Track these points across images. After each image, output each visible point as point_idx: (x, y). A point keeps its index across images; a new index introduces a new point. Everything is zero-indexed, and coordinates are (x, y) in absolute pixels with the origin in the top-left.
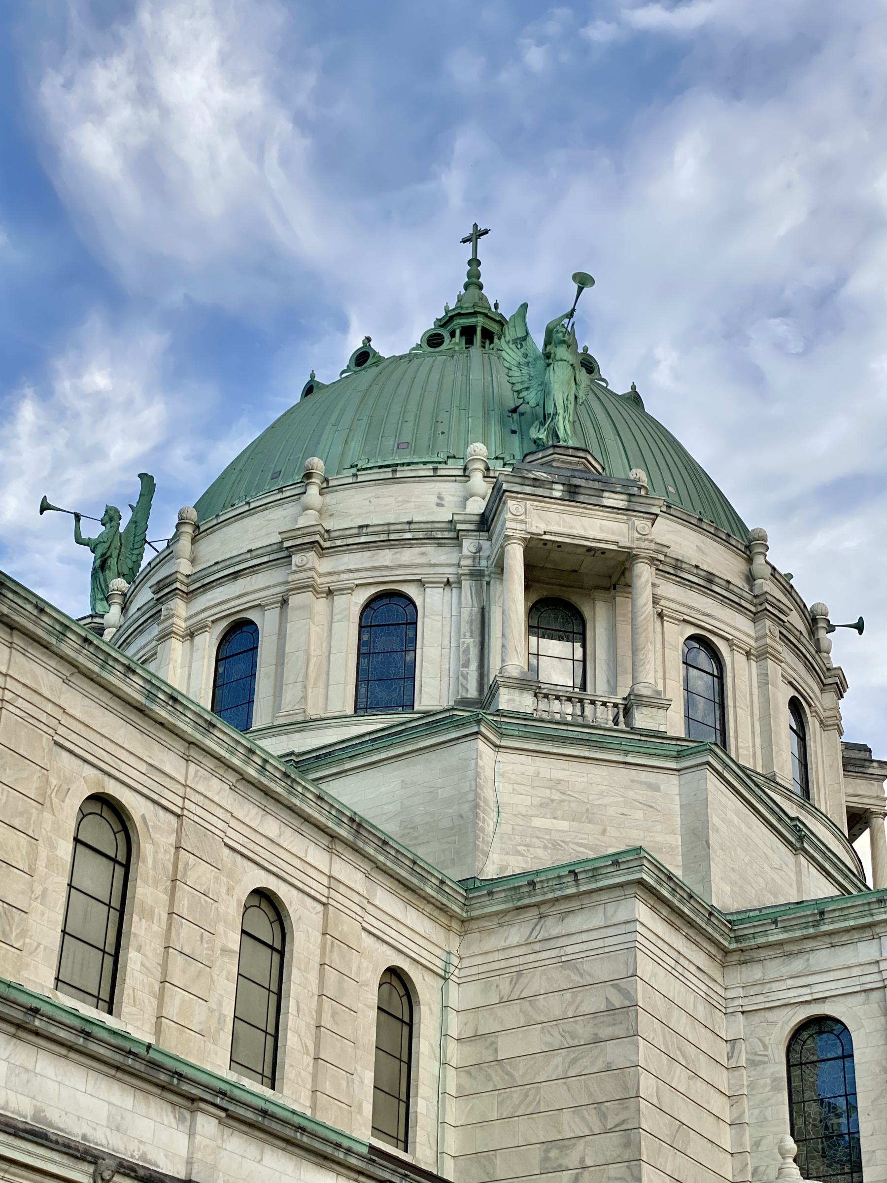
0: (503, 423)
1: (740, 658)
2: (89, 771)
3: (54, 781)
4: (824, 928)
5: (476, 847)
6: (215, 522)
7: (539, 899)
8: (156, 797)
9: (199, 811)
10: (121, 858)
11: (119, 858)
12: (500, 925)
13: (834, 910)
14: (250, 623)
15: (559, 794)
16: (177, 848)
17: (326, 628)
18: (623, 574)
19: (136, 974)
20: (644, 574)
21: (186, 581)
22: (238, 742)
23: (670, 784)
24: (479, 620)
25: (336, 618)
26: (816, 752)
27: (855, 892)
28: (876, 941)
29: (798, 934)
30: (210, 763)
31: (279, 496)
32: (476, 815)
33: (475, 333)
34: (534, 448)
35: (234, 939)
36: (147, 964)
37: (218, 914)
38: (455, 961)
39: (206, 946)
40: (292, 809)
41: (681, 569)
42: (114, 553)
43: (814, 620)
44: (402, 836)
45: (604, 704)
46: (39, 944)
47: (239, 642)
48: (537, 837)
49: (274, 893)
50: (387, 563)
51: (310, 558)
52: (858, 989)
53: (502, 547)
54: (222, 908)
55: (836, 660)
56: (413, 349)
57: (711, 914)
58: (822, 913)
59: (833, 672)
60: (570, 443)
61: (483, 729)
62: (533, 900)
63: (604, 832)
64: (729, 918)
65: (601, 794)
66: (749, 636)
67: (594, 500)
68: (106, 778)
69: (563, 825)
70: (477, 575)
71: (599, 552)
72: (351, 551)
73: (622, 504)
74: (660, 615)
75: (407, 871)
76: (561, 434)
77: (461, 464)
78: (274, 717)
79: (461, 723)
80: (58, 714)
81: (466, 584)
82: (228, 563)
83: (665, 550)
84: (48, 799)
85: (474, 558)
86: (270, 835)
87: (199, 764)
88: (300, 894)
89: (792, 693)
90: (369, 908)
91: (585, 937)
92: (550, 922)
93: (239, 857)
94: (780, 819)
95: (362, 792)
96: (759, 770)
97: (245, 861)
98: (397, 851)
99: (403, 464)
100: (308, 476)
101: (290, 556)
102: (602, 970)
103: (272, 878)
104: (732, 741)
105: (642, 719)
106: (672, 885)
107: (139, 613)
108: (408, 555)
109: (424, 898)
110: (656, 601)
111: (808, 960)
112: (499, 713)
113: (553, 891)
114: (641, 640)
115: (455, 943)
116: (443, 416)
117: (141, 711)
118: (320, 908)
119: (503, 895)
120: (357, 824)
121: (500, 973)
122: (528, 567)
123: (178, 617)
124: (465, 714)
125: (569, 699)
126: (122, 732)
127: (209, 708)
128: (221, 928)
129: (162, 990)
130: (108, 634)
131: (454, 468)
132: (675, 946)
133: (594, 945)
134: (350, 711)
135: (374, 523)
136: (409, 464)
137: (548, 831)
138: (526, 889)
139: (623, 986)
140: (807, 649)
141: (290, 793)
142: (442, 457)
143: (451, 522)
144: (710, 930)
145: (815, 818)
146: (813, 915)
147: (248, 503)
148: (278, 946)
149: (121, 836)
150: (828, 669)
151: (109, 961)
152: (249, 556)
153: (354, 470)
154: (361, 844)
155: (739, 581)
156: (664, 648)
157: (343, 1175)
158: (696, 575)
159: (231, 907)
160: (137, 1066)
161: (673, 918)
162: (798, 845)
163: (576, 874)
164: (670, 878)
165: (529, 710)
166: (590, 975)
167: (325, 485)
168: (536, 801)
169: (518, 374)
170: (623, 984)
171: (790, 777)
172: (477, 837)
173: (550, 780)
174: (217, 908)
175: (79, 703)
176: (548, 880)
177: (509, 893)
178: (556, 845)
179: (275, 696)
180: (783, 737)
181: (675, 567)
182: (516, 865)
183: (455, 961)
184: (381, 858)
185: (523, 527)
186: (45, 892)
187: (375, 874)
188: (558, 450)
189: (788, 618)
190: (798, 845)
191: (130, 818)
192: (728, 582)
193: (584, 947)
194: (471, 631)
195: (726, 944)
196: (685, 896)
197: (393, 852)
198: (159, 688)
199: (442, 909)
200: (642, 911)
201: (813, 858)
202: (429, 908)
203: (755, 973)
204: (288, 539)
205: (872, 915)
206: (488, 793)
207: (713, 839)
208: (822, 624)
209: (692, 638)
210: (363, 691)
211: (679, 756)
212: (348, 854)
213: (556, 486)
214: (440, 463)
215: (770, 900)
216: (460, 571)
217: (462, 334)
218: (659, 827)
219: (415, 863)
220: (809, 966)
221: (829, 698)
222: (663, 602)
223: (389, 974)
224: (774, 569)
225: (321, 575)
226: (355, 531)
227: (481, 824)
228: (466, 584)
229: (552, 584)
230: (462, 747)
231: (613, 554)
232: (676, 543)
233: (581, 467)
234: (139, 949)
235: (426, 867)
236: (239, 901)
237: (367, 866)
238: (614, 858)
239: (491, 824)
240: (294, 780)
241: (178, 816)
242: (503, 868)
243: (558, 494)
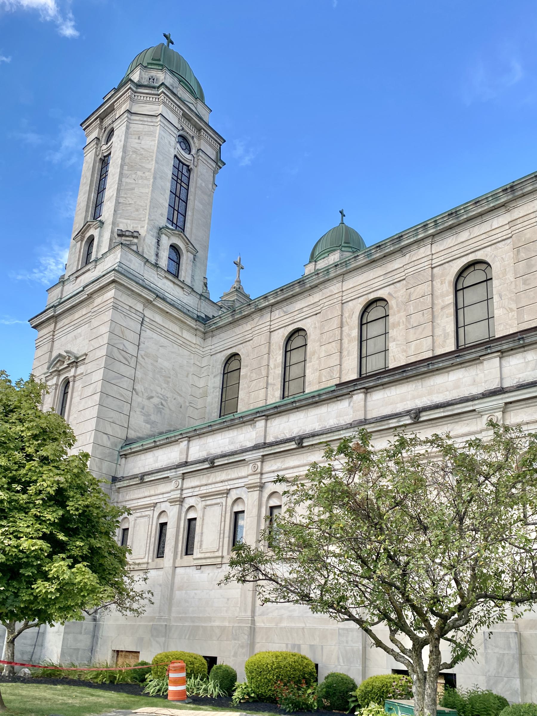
157: (330, 403)
160: (228, 424)
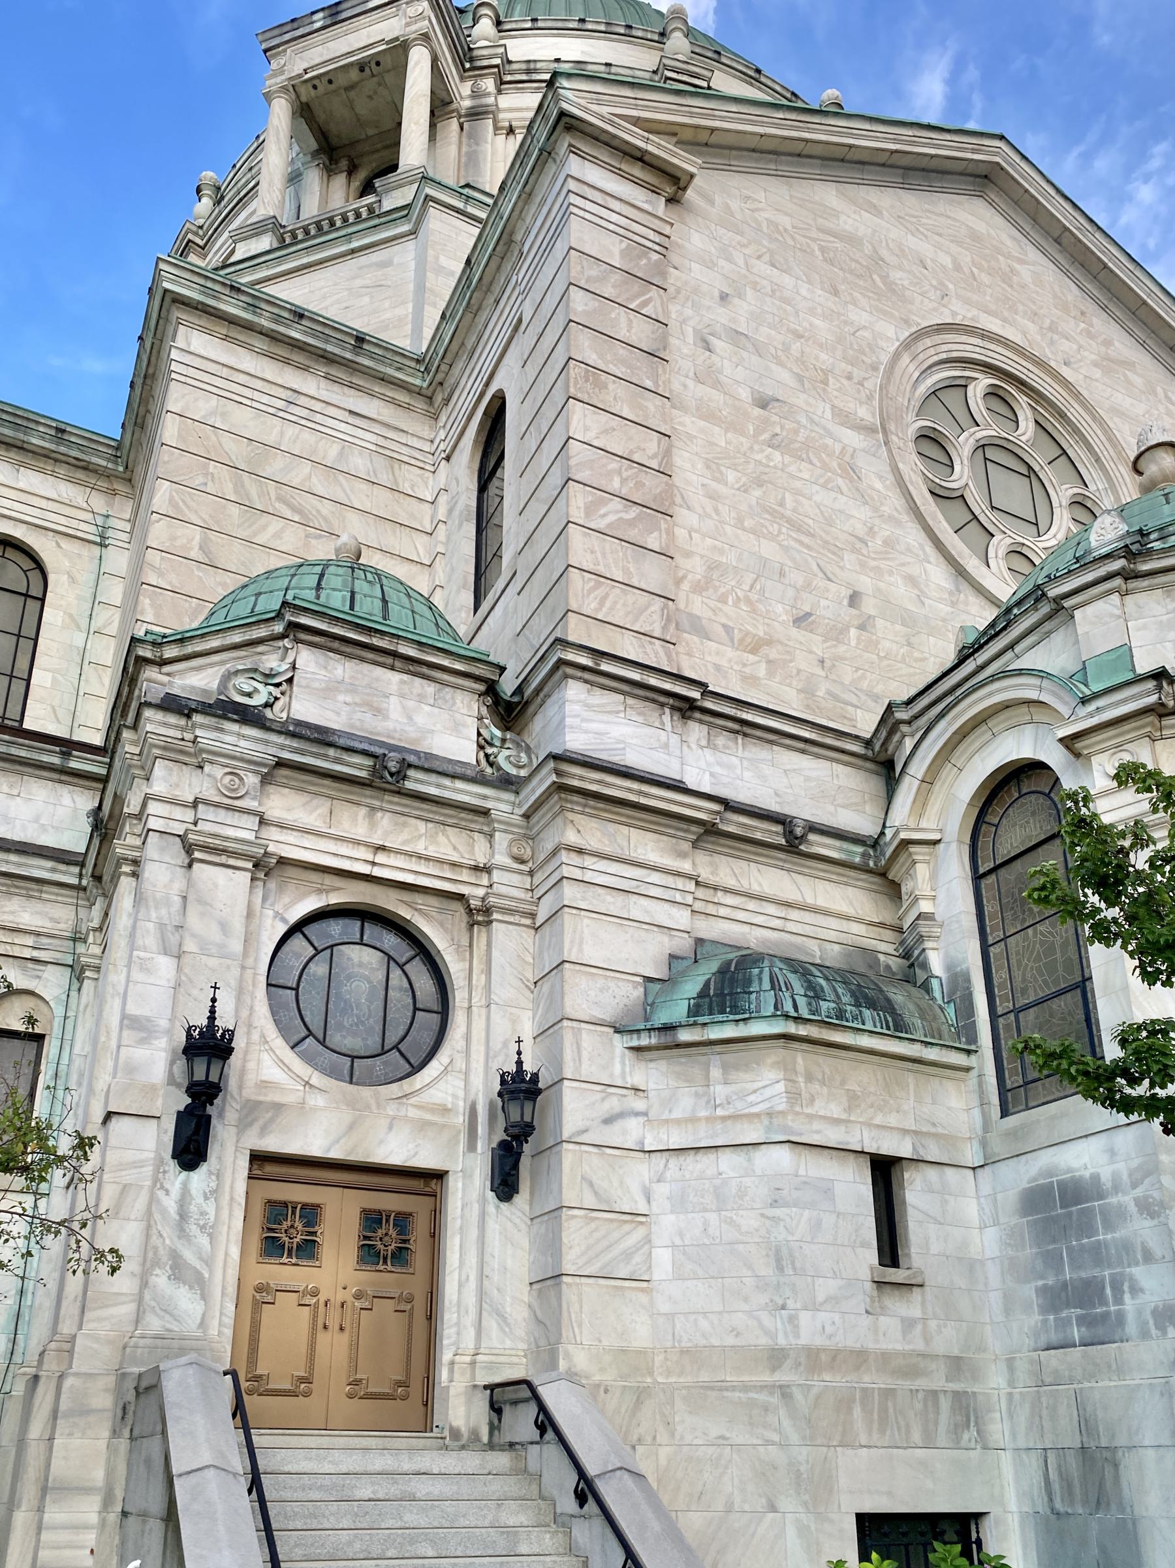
41: (536, 71)
71: (373, 65)
144: (367, 362)
181: (528, 71)
195: (418, 382)
229: (378, 151)
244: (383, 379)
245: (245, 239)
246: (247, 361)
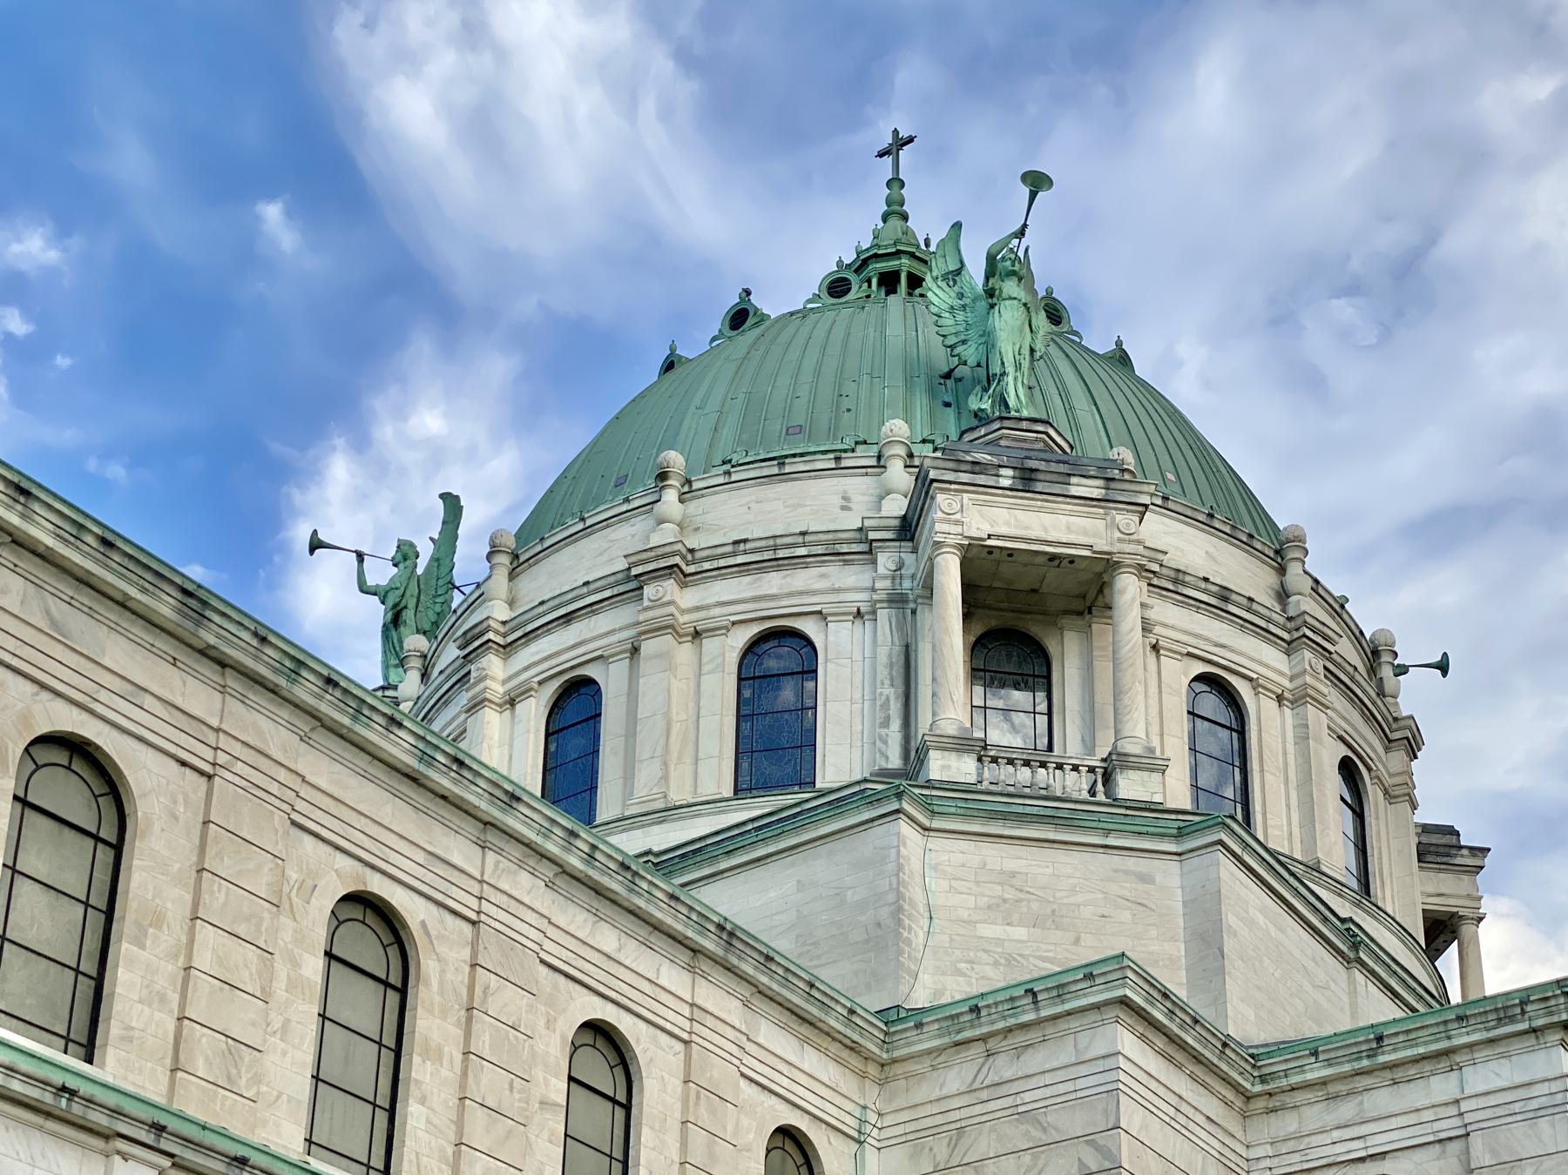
0: (932, 393)
1: (1269, 705)
2: (342, 861)
3: (294, 876)
4: (1382, 1059)
5: (900, 965)
6: (539, 548)
7: (985, 1030)
8: (440, 897)
9: (502, 916)
10: (395, 979)
11: (392, 980)
12: (934, 1068)
13: (1397, 1034)
14: (590, 682)
15: (1013, 891)
16: (473, 966)
17: (692, 684)
18: (1101, 591)
19: (420, 1134)
20: (1129, 589)
21: (502, 629)
22: (553, 821)
23: (1168, 874)
24: (902, 662)
25: (706, 669)
26: (1379, 833)
27: (1421, 1008)
28: (1455, 1074)
29: (1347, 1068)
30: (516, 851)
31: (625, 508)
32: (899, 922)
33: (898, 280)
34: (975, 422)
35: (558, 1088)
36: (435, 1121)
37: (534, 1054)
38: (872, 1118)
39: (517, 1096)
40: (634, 913)
41: (1184, 583)
42: (416, 602)
43: (1376, 653)
44: (800, 955)
45: (1075, 768)
46: (280, 1094)
47: (575, 706)
48: (985, 951)
49: (615, 1028)
50: (774, 591)
51: (668, 588)
52: (1431, 1138)
53: (931, 559)
54: (540, 1047)
55: (1405, 707)
56: (809, 301)
57: (1225, 1045)
58: (1380, 1039)
59: (1402, 723)
60: (1025, 413)
61: (906, 806)
62: (977, 1032)
63: (1077, 941)
64: (1251, 1051)
65: (1073, 891)
66: (1281, 673)
67: (1057, 489)
68: (368, 871)
69: (1020, 932)
70: (897, 600)
72: (723, 577)
73: (1097, 493)
74: (1155, 648)
75: (802, 997)
76: (1012, 402)
77: (874, 450)
78: (624, 806)
79: (877, 799)
80: (295, 783)
81: (883, 614)
82: (557, 601)
83: (1160, 556)
84: (285, 898)
85: (893, 578)
86: (606, 949)
87: (499, 852)
88: (651, 1029)
89: (1344, 751)
90: (750, 1047)
91: (1048, 1079)
92: (1000, 1060)
93: (562, 978)
94: (1325, 920)
95: (747, 899)
96: (1298, 856)
97: (571, 984)
98: (787, 970)
99: (794, 456)
100: (663, 476)
101: (641, 588)
102: (1075, 1122)
103: (610, 1006)
104: (1258, 818)
105: (1130, 786)
106: (1168, 1004)
107: (442, 677)
108: (802, 579)
109: (828, 1034)
110: (1147, 628)
111: (1362, 1103)
112: (929, 785)
113: (1004, 1018)
114: (1126, 679)
115: (872, 1095)
116: (849, 388)
117: (414, 780)
118: (679, 1046)
119: (936, 1026)
120: (728, 933)
121: (934, 1132)
122: (968, 587)
123: (493, 678)
124: (880, 787)
125: (1027, 763)
126: (389, 809)
127: (539, 794)
128: (539, 1074)
129: (457, 1155)
130: (405, 707)
131: (865, 456)
132: (1175, 1088)
133: (1062, 1088)
134: (728, 792)
135: (756, 536)
136: (802, 455)
137: (999, 942)
138: (968, 1017)
139: (1101, 1142)
140: (1364, 691)
141: (631, 891)
142: (849, 442)
143: (860, 530)
145: (1380, 922)
146: (1368, 1041)
147: (583, 519)
148: (621, 1097)
149: (393, 951)
150: (1396, 719)
151: (382, 1117)
152: (585, 590)
153: (727, 467)
154: (735, 961)
155: (1266, 599)
156: (1160, 692)
158: (1204, 591)
159: (553, 1045)
161: (1171, 1050)
162: (1352, 955)
163: (1035, 994)
164: (1165, 996)
165: (973, 779)
166: (1057, 1129)
167: (686, 489)
168: (983, 901)
169: (951, 322)
170: (1101, 1139)
171: (1342, 865)
172: (900, 952)
173: (1002, 872)
174: (532, 1047)
175: (324, 769)
176: (996, 1004)
177: (944, 1024)
178: (1010, 961)
179: (625, 778)
180: (1331, 811)
181: (1175, 581)
182: (957, 989)
183: (872, 1118)
184: (764, 979)
185: (959, 529)
186: (286, 1025)
187: (757, 1001)
188: (1007, 423)
189: (1337, 648)
190: (1352, 955)
191: (405, 926)
192: (1251, 599)
193: (1048, 1092)
194: (892, 679)
195: (1248, 1086)
196: (1188, 1020)
197: (780, 971)
198: (437, 748)
199: (853, 1048)
200: (1126, 1040)
201: (1373, 972)
202: (834, 1048)
203: (1288, 1123)
204: (636, 564)
205: (1449, 1038)
206: (915, 893)
207: (1229, 945)
208: (1385, 658)
209: (1200, 678)
210: (745, 765)
211: (1180, 834)
212: (718, 975)
213: (1003, 471)
214: (845, 451)
215: (1311, 1030)
216: (875, 597)
217: (880, 284)
218: (1154, 932)
219: (812, 986)
220: (1362, 1111)
221: (1397, 758)
222: (1158, 629)
223: (780, 1137)
224: (1317, 582)
225: (683, 612)
226: (729, 549)
227: (906, 934)
228: (883, 614)
230: (878, 831)
231: (1084, 564)
232: (1177, 549)
233: (1040, 445)
234: (423, 1101)
235: (828, 991)
236: (563, 1037)
237: (746, 991)
238: (1087, 970)
239: (921, 935)
240: (636, 874)
241: (474, 923)
242: (938, 993)
243: (1006, 483)
244: (1226, 1080)
245: (945, 749)
246: (1182, 1084)
